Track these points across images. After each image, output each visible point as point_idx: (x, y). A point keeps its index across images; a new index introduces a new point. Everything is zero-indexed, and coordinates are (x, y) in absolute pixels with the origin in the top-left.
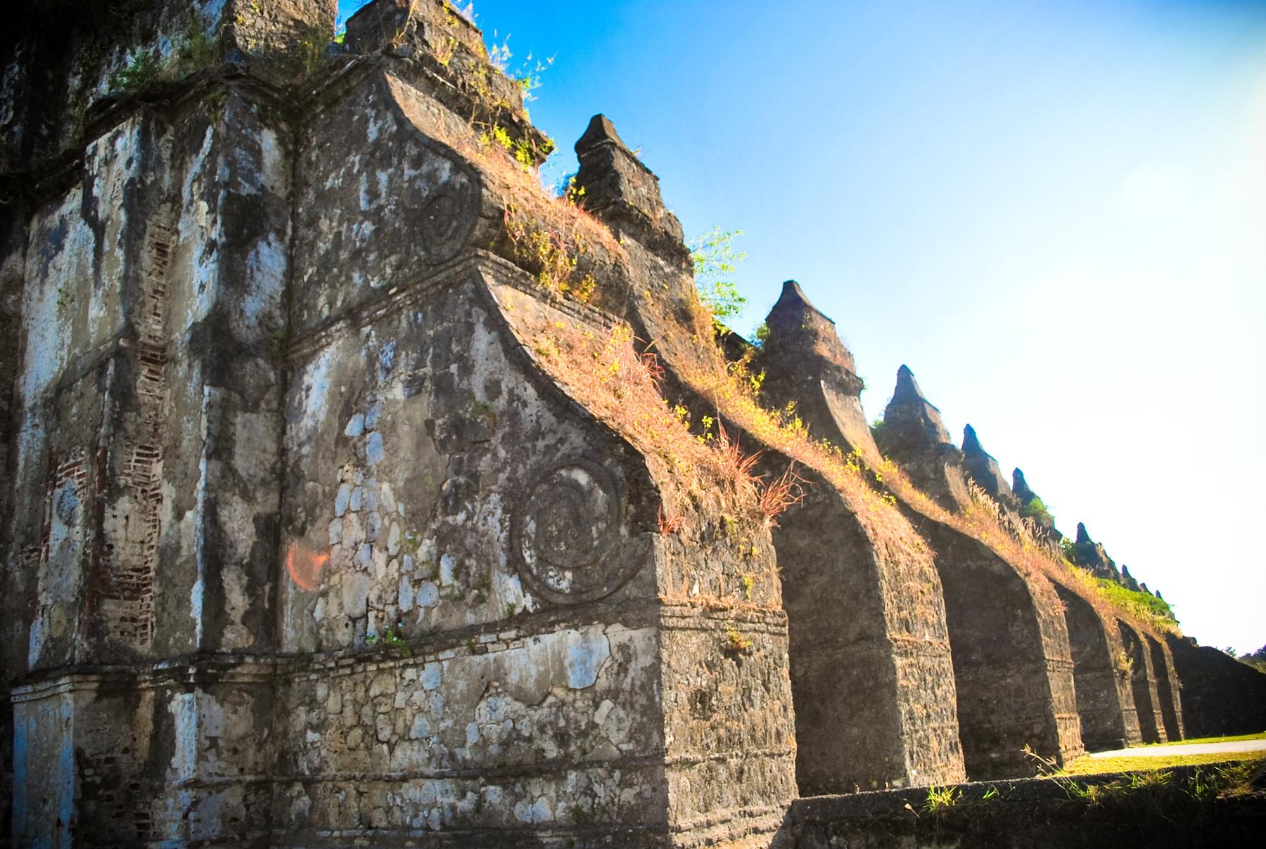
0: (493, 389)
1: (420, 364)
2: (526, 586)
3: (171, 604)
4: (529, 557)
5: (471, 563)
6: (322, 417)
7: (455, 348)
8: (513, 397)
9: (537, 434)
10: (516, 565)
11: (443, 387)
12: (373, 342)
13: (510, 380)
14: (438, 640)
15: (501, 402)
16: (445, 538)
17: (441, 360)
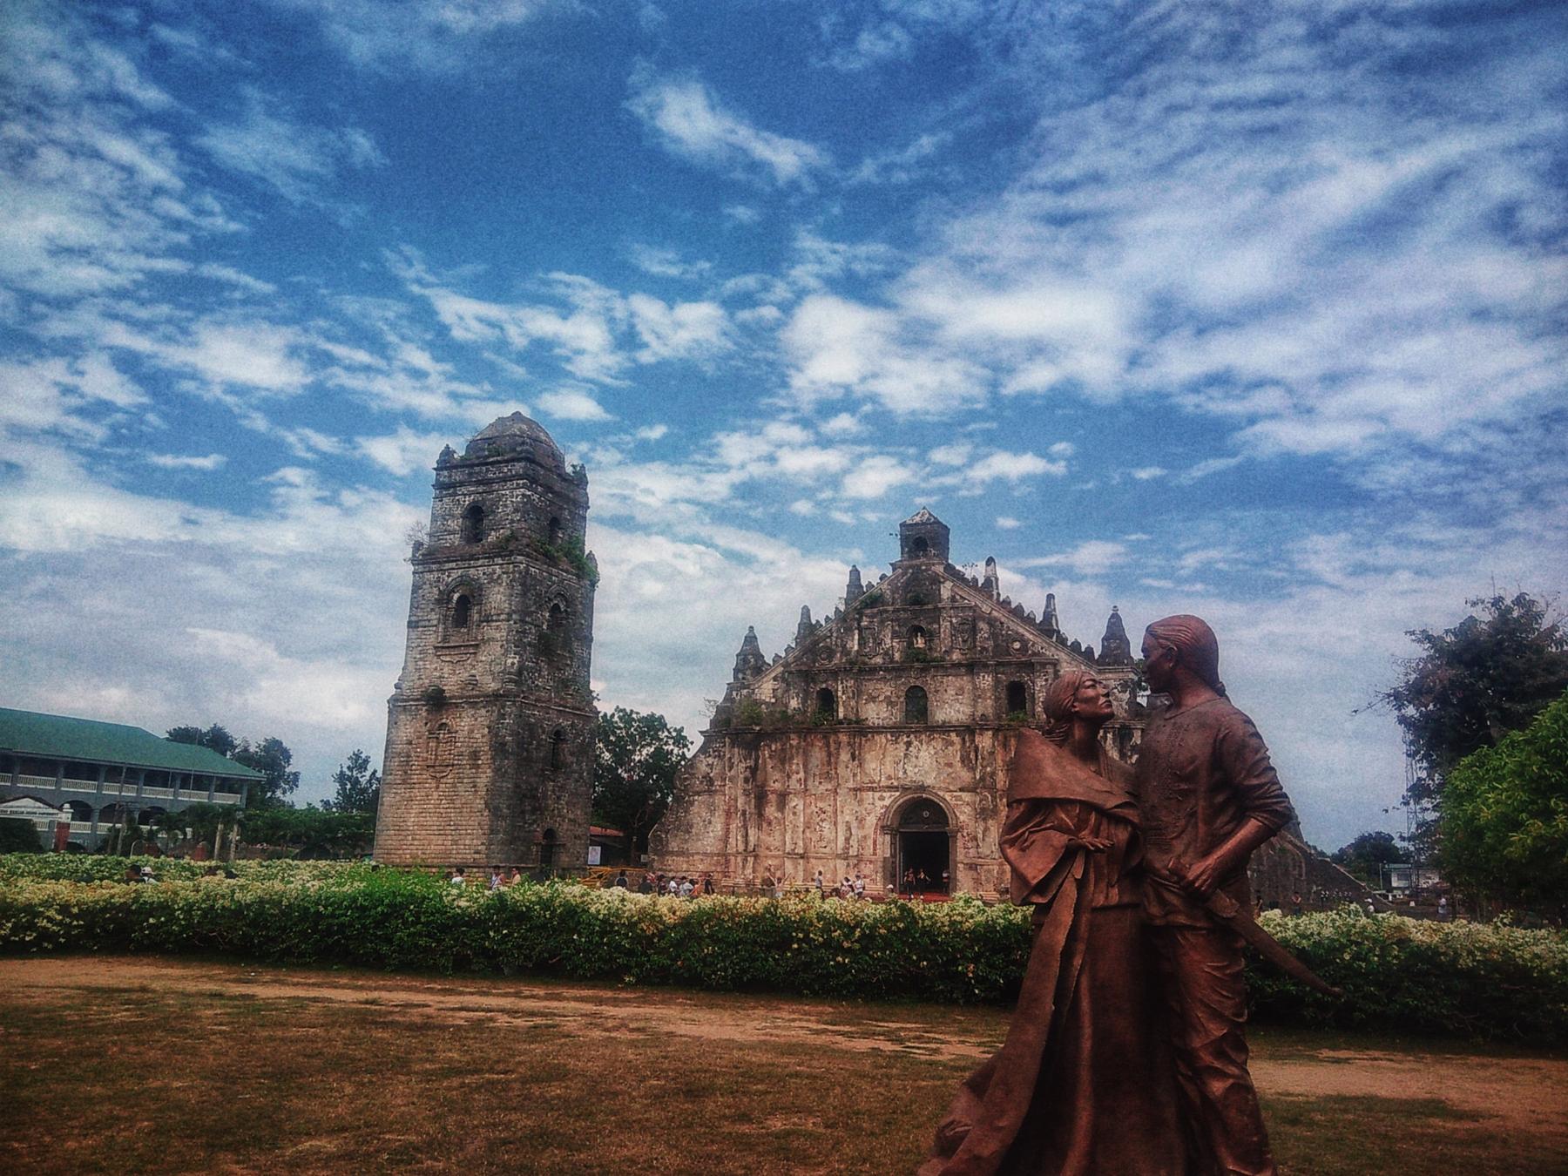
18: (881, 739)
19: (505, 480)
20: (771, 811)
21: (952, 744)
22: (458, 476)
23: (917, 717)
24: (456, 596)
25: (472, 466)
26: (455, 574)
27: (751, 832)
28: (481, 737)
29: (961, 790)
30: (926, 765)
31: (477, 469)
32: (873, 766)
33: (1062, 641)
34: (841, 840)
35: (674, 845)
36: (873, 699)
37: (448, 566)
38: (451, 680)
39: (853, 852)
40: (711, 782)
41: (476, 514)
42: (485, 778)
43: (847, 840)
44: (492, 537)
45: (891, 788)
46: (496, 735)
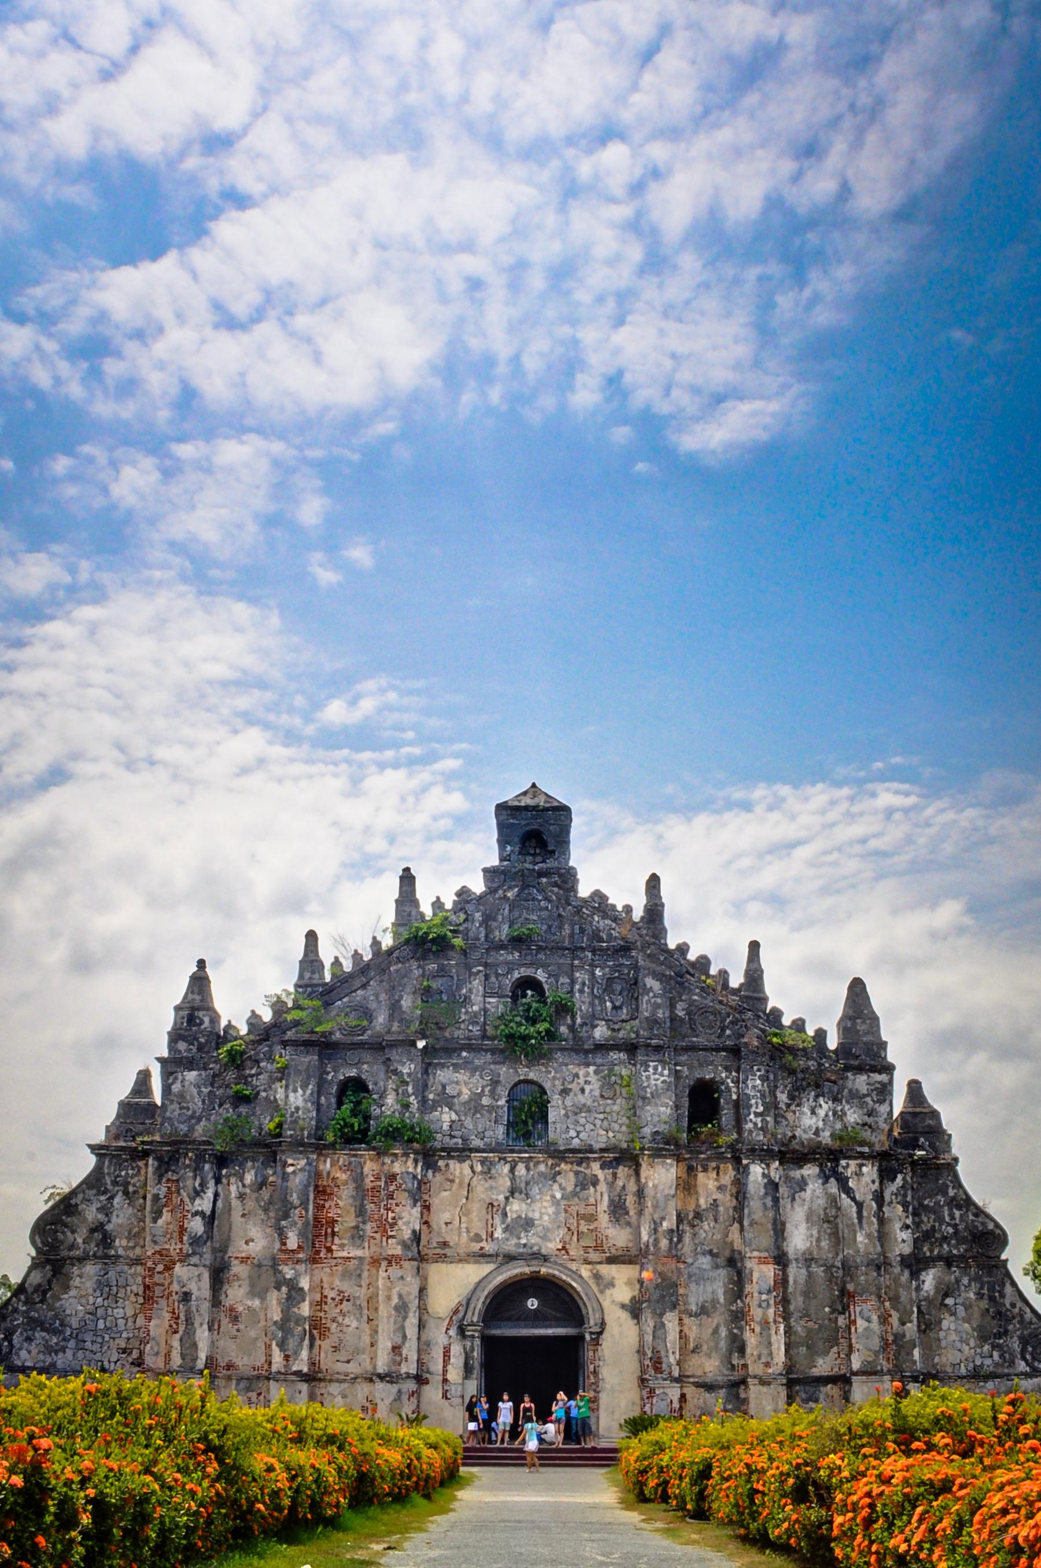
0: (1013, 1305)
1: (981, 1288)
2: (1028, 1364)
3: (903, 1354)
4: (1028, 1357)
5: (1007, 1356)
6: (932, 1293)
7: (997, 1288)
8: (1020, 1309)
9: (1031, 1323)
10: (1024, 1358)
11: (992, 1299)
12: (957, 1274)
13: (1019, 1304)
14: (993, 1376)
15: (1016, 1310)
16: (994, 1347)
17: (992, 1289)
18: (459, 1169)
20: (236, 1294)
21: (595, 1182)
27: (202, 1335)
29: (611, 1260)
30: (546, 1217)
32: (446, 1216)
33: (777, 1014)
34: (385, 1344)
36: (446, 1100)
40: (107, 1240)
43: (396, 1349)
45: (482, 1256)
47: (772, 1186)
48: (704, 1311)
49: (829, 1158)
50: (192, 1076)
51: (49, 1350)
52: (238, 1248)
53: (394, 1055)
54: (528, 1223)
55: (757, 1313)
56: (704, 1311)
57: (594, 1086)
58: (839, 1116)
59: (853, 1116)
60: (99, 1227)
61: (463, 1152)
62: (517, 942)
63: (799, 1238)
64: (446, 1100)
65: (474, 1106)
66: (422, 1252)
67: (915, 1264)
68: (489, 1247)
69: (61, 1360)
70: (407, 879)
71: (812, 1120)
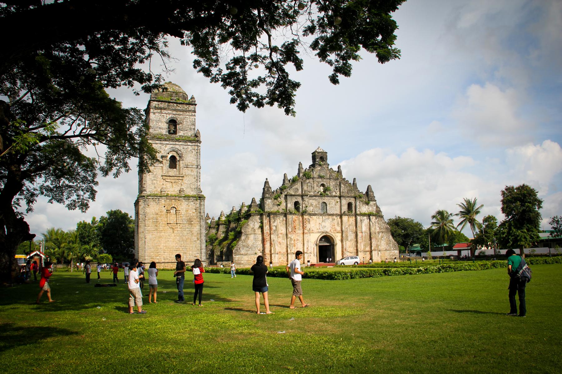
19: (186, 111)
22: (162, 105)
23: (324, 212)
24: (169, 156)
25: (169, 102)
26: (169, 147)
27: (276, 247)
28: (192, 212)
31: (172, 104)
35: (243, 252)
37: (164, 142)
38: (173, 190)
39: (309, 251)
40: (255, 230)
41: (173, 122)
42: (196, 229)
43: (307, 248)
44: (180, 133)
46: (200, 213)
47: (361, 220)
48: (351, 241)
49: (369, 215)
50: (270, 201)
51: (247, 251)
52: (280, 232)
53: (305, 197)
54: (325, 227)
55: (359, 241)
56: (351, 241)
57: (334, 203)
58: (369, 208)
59: (371, 209)
60: (253, 228)
61: (315, 215)
62: (320, 177)
63: (364, 229)
64: (312, 205)
65: (316, 206)
66: (310, 232)
67: (379, 233)
68: (320, 231)
69: (249, 252)
70: (300, 164)
71: (365, 209)
